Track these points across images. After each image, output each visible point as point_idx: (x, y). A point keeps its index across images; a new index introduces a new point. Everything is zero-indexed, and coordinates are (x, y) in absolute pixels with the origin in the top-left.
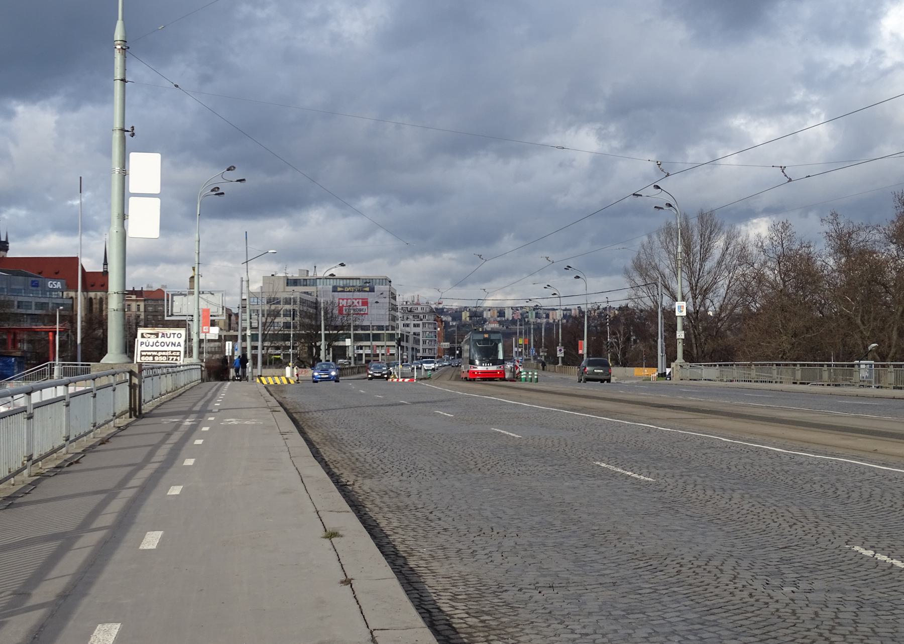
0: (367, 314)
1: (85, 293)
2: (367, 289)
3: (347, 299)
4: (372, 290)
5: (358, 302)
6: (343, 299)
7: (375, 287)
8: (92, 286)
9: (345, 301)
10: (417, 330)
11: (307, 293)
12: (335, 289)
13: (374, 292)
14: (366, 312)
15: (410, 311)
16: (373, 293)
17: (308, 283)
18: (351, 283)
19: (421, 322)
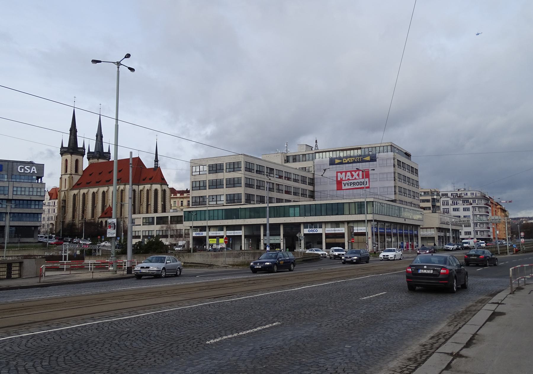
0: (368, 187)
1: (135, 187)
2: (368, 158)
3: (346, 172)
4: (373, 159)
5: (358, 175)
6: (341, 173)
7: (377, 154)
8: (144, 180)
9: (344, 174)
10: (467, 213)
11: (304, 169)
12: (332, 162)
14: (368, 185)
15: (460, 197)
16: (375, 163)
17: (307, 158)
18: (352, 153)
19: (470, 206)
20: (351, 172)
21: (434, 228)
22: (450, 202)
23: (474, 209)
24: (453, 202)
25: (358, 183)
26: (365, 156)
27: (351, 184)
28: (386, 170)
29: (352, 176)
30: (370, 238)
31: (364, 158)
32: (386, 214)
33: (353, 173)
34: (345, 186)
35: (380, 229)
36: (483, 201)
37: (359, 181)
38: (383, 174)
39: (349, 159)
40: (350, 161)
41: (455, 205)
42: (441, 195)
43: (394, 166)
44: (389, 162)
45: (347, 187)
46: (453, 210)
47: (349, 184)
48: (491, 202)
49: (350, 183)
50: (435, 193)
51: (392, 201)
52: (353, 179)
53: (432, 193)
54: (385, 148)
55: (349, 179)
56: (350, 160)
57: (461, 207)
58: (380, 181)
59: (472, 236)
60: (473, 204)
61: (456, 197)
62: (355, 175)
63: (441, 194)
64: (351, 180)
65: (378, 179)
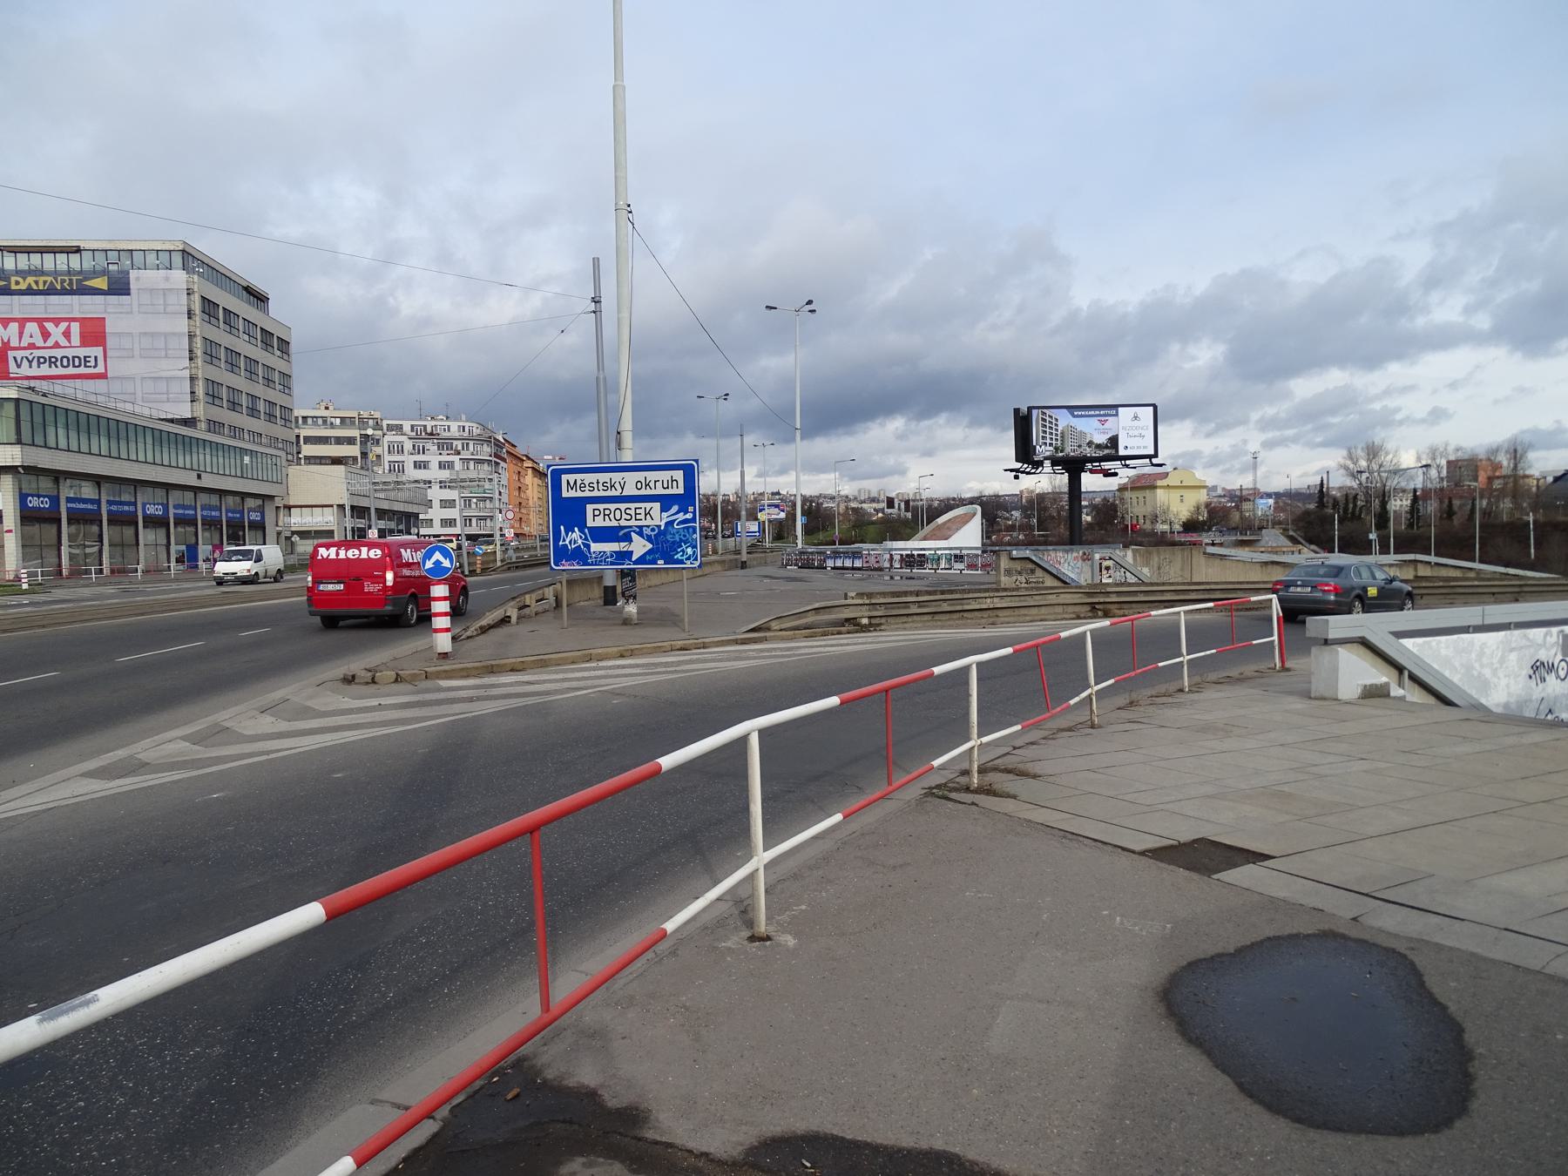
0: (103, 376)
3: (22, 322)
4: (120, 287)
5: (67, 334)
7: (133, 274)
9: (14, 327)
13: (129, 294)
14: (100, 369)
15: (432, 434)
19: (456, 458)
20: (40, 321)
21: (332, 506)
22: (408, 445)
23: (463, 466)
24: (414, 446)
25: (65, 360)
26: (95, 274)
27: (41, 361)
28: (163, 325)
29: (46, 335)
30: (10, 531)
31: (86, 279)
32: (265, 479)
33: (49, 326)
34: (19, 366)
35: (176, 507)
36: (485, 446)
37: (70, 353)
38: (153, 335)
39: (34, 278)
40: (35, 287)
41: (419, 453)
42: (385, 428)
43: (190, 314)
44: (172, 299)
45: (25, 370)
46: (415, 467)
47: (35, 364)
48: (507, 452)
49: (39, 358)
50: (371, 422)
51: (186, 422)
52: (48, 344)
53: (363, 422)
54: (164, 257)
55: (32, 346)
56: (37, 283)
57: (434, 458)
58: (141, 357)
59: (457, 530)
60: (462, 452)
61: (423, 434)
62: (56, 332)
63: (385, 423)
64: (39, 348)
65: (137, 353)
